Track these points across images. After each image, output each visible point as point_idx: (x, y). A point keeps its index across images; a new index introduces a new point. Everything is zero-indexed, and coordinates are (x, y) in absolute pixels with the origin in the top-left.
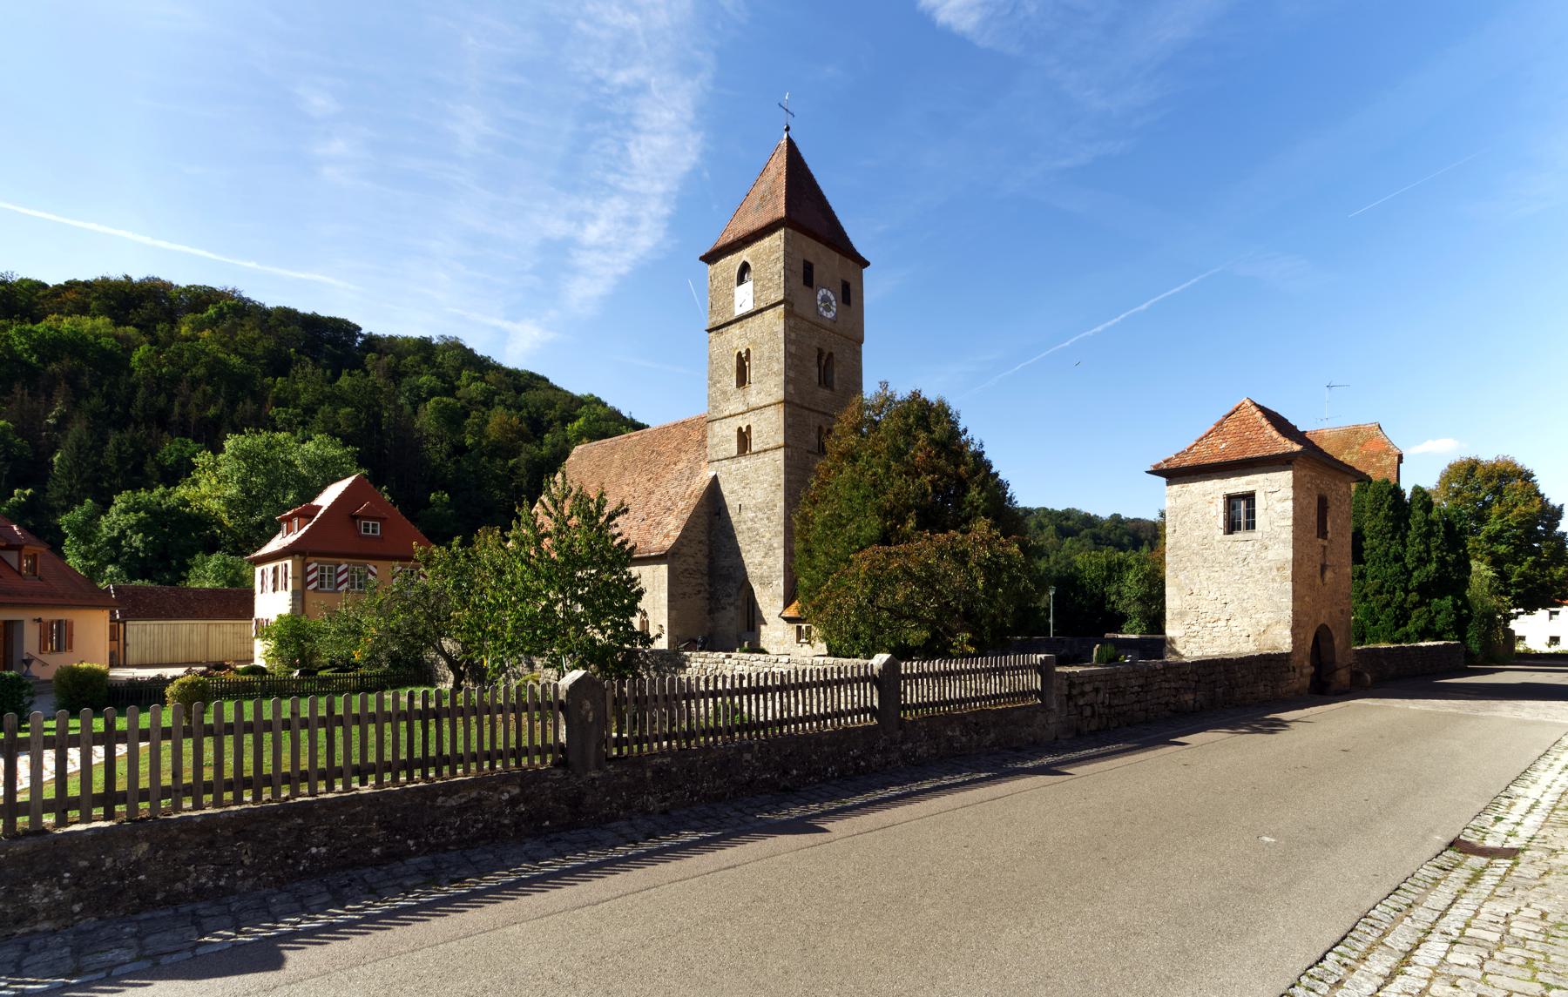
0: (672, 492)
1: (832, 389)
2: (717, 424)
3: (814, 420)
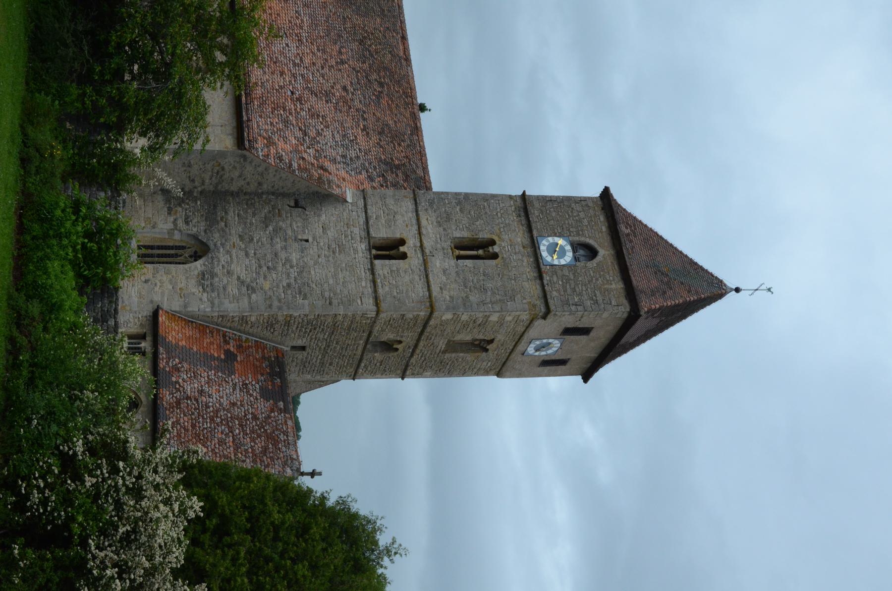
0: (328, 133)
1: (445, 352)
2: (410, 205)
3: (409, 338)
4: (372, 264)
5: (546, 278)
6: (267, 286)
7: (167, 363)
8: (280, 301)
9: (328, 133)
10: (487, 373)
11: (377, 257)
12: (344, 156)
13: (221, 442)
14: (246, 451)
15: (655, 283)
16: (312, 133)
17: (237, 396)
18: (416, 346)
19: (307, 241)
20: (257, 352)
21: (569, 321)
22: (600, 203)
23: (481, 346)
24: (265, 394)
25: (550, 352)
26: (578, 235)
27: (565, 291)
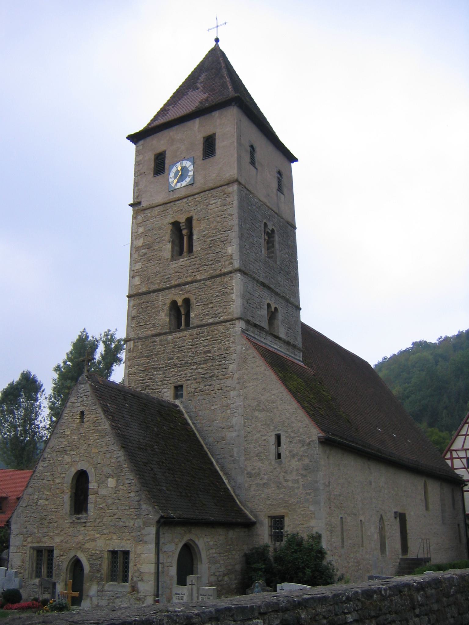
18: (179, 285)
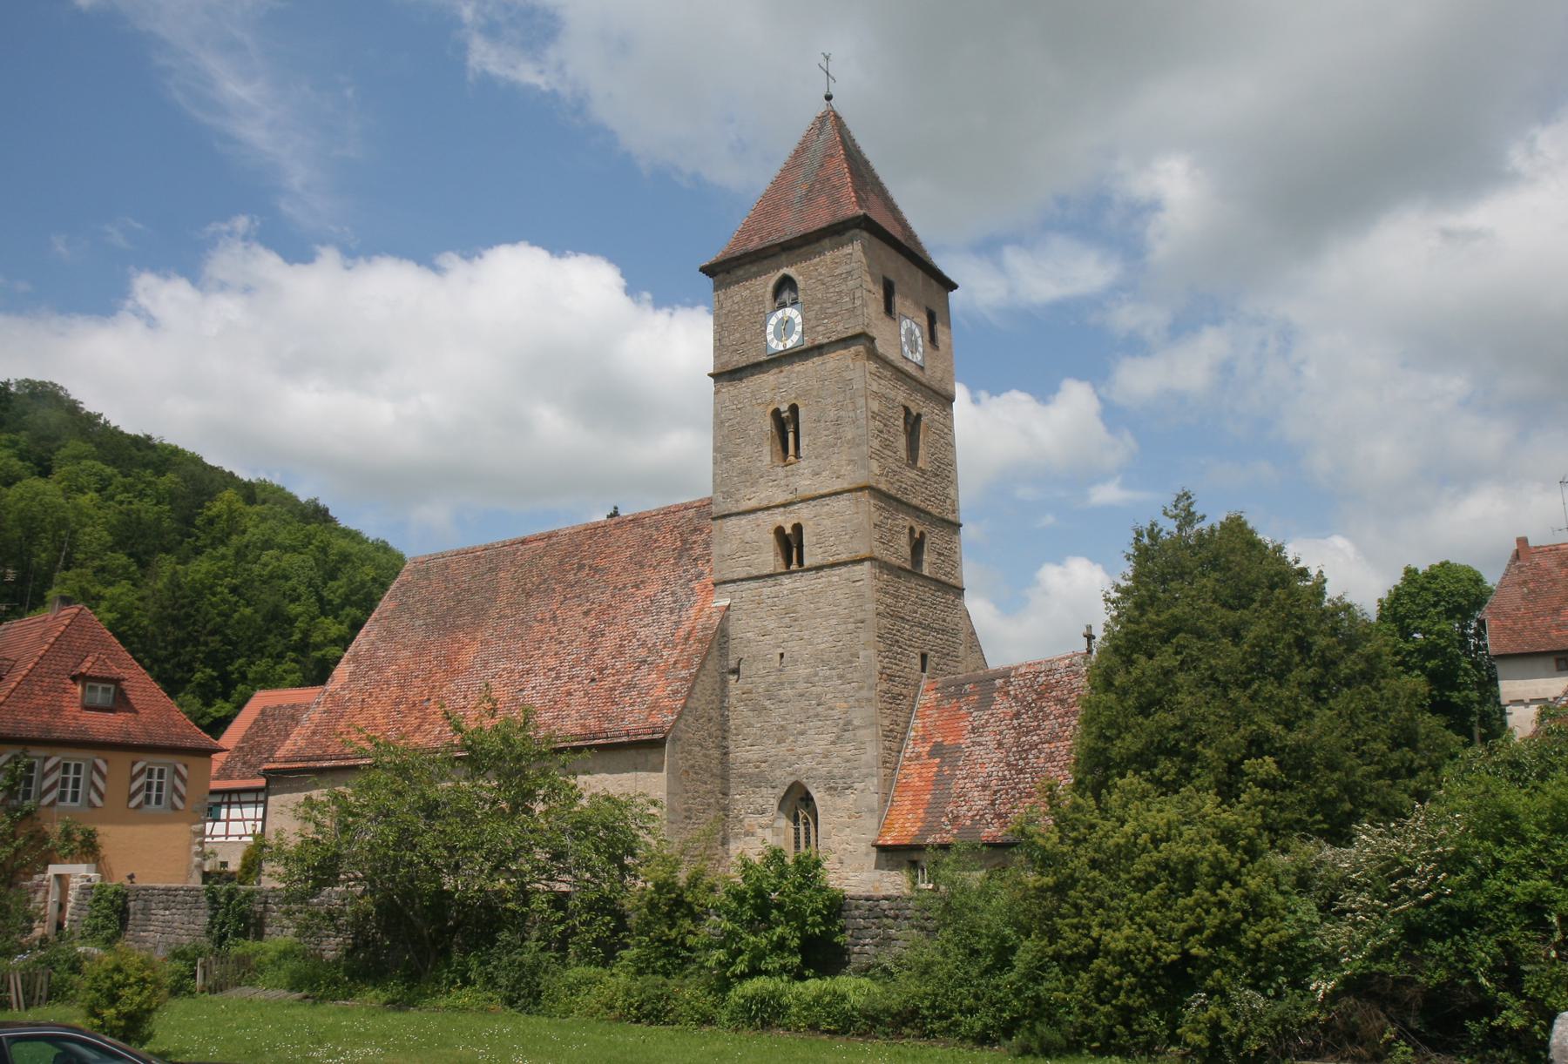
0: (643, 633)
3: (904, 521)
4: (809, 570)
5: (821, 340)
6: (841, 705)
7: (947, 832)
8: (861, 688)
9: (643, 633)
10: (950, 416)
11: (800, 562)
12: (672, 613)
13: (1051, 758)
14: (1061, 725)
15: (822, 200)
16: (642, 653)
17: (989, 739)
19: (782, 655)
20: (929, 716)
21: (876, 306)
22: (721, 276)
23: (913, 423)
24: (985, 703)
25: (917, 333)
26: (762, 302)
27: (836, 314)
